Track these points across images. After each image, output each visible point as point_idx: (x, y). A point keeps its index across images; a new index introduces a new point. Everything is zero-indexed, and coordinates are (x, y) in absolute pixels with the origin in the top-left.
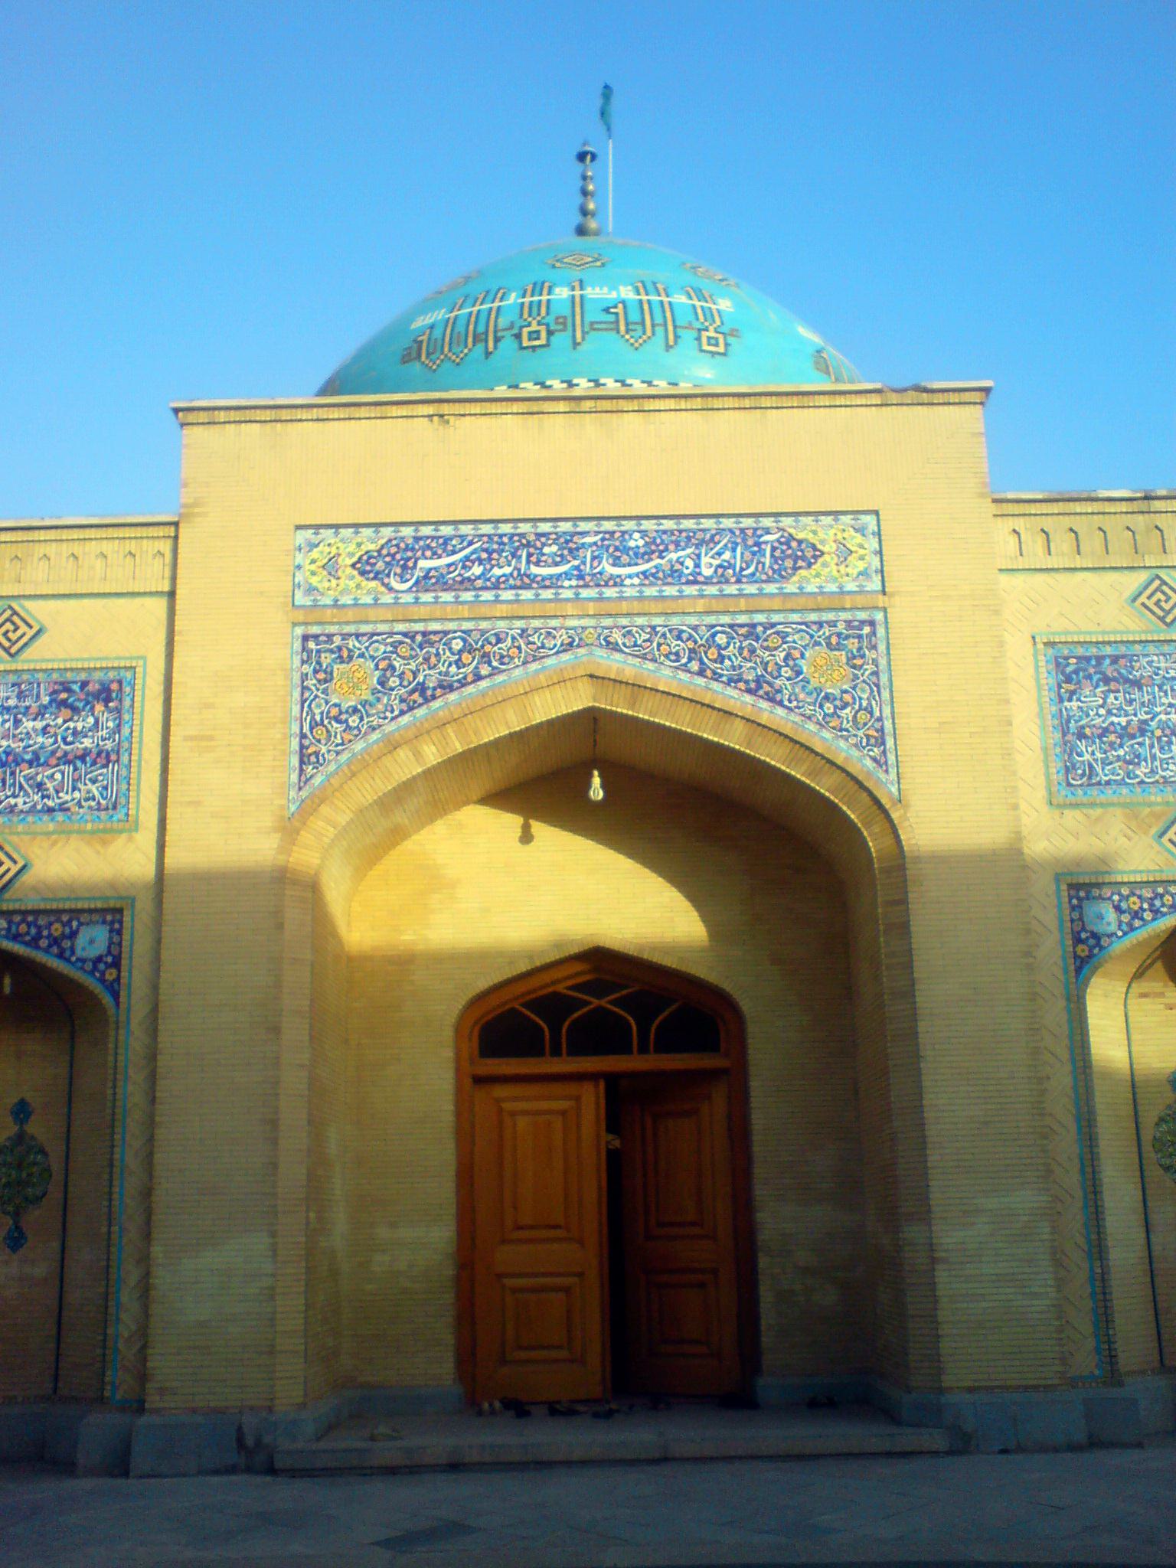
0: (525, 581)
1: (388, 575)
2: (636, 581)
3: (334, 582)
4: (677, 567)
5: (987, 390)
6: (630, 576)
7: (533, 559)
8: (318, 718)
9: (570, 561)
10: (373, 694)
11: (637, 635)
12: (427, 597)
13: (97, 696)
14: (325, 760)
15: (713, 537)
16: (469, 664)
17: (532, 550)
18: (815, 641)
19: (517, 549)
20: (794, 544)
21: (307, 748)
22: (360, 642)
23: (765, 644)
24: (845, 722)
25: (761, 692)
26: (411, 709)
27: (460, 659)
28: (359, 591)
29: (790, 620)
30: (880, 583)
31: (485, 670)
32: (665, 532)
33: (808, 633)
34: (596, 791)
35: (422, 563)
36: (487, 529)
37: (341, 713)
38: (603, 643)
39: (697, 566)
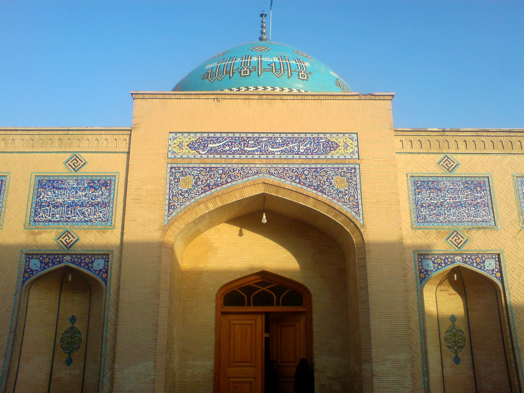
0: (243, 152)
1: (199, 149)
2: (279, 153)
3: (181, 150)
4: (292, 149)
5: (393, 96)
6: (277, 152)
7: (246, 145)
8: (175, 194)
9: (257, 146)
10: (193, 187)
11: (279, 170)
12: (211, 156)
13: (103, 185)
14: (176, 207)
15: (304, 140)
16: (224, 178)
17: (245, 142)
18: (337, 174)
19: (241, 142)
20: (330, 143)
21: (171, 203)
22: (189, 170)
23: (320, 174)
24: (346, 200)
25: (319, 190)
26: (205, 192)
27: (221, 176)
28: (189, 154)
29: (328, 167)
30: (358, 156)
31: (229, 180)
32: (288, 138)
33: (334, 171)
34: (264, 220)
35: (210, 145)
36: (231, 135)
37: (182, 192)
38: (268, 172)
39: (298, 149)
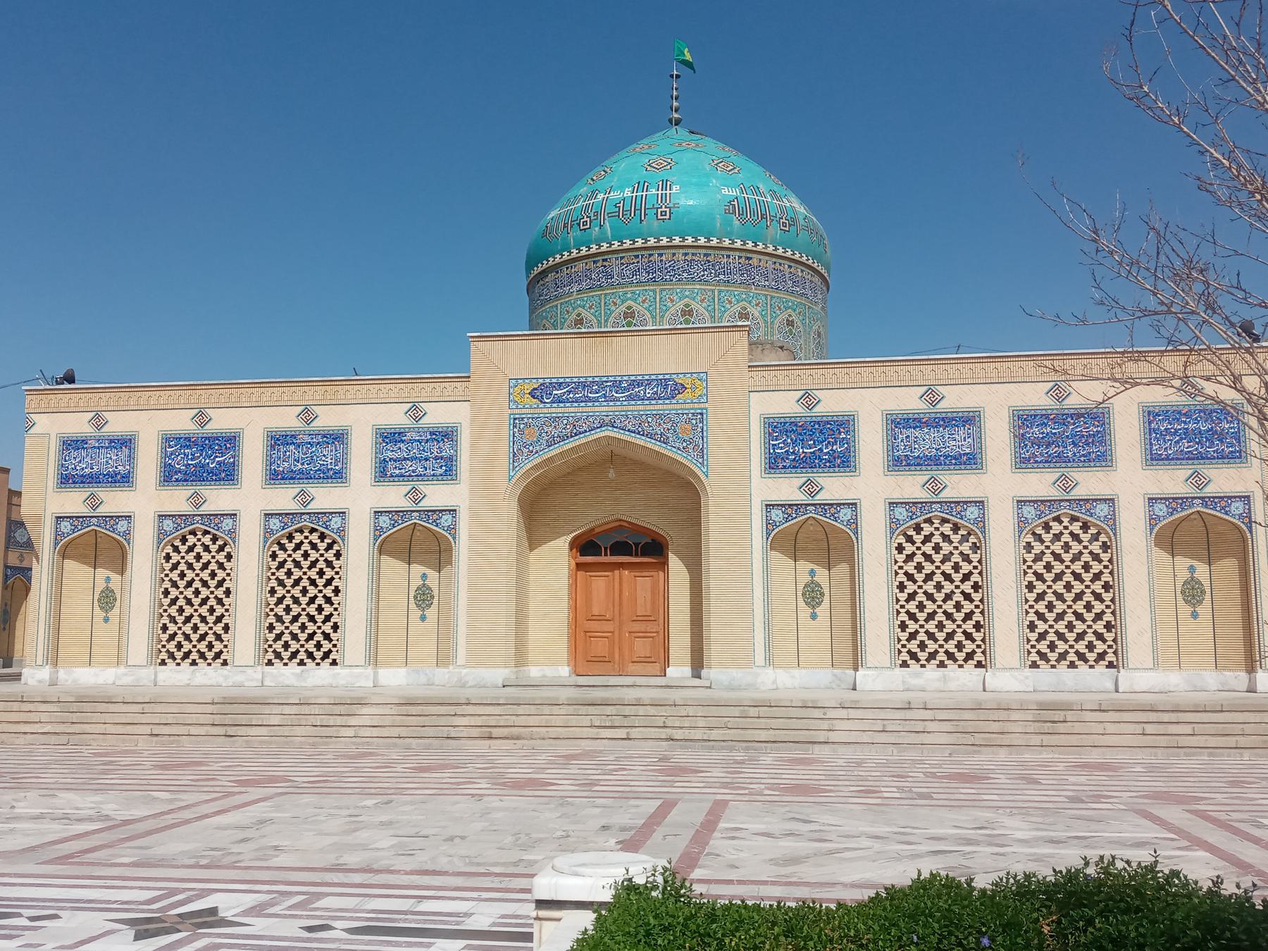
39: (645, 393)
